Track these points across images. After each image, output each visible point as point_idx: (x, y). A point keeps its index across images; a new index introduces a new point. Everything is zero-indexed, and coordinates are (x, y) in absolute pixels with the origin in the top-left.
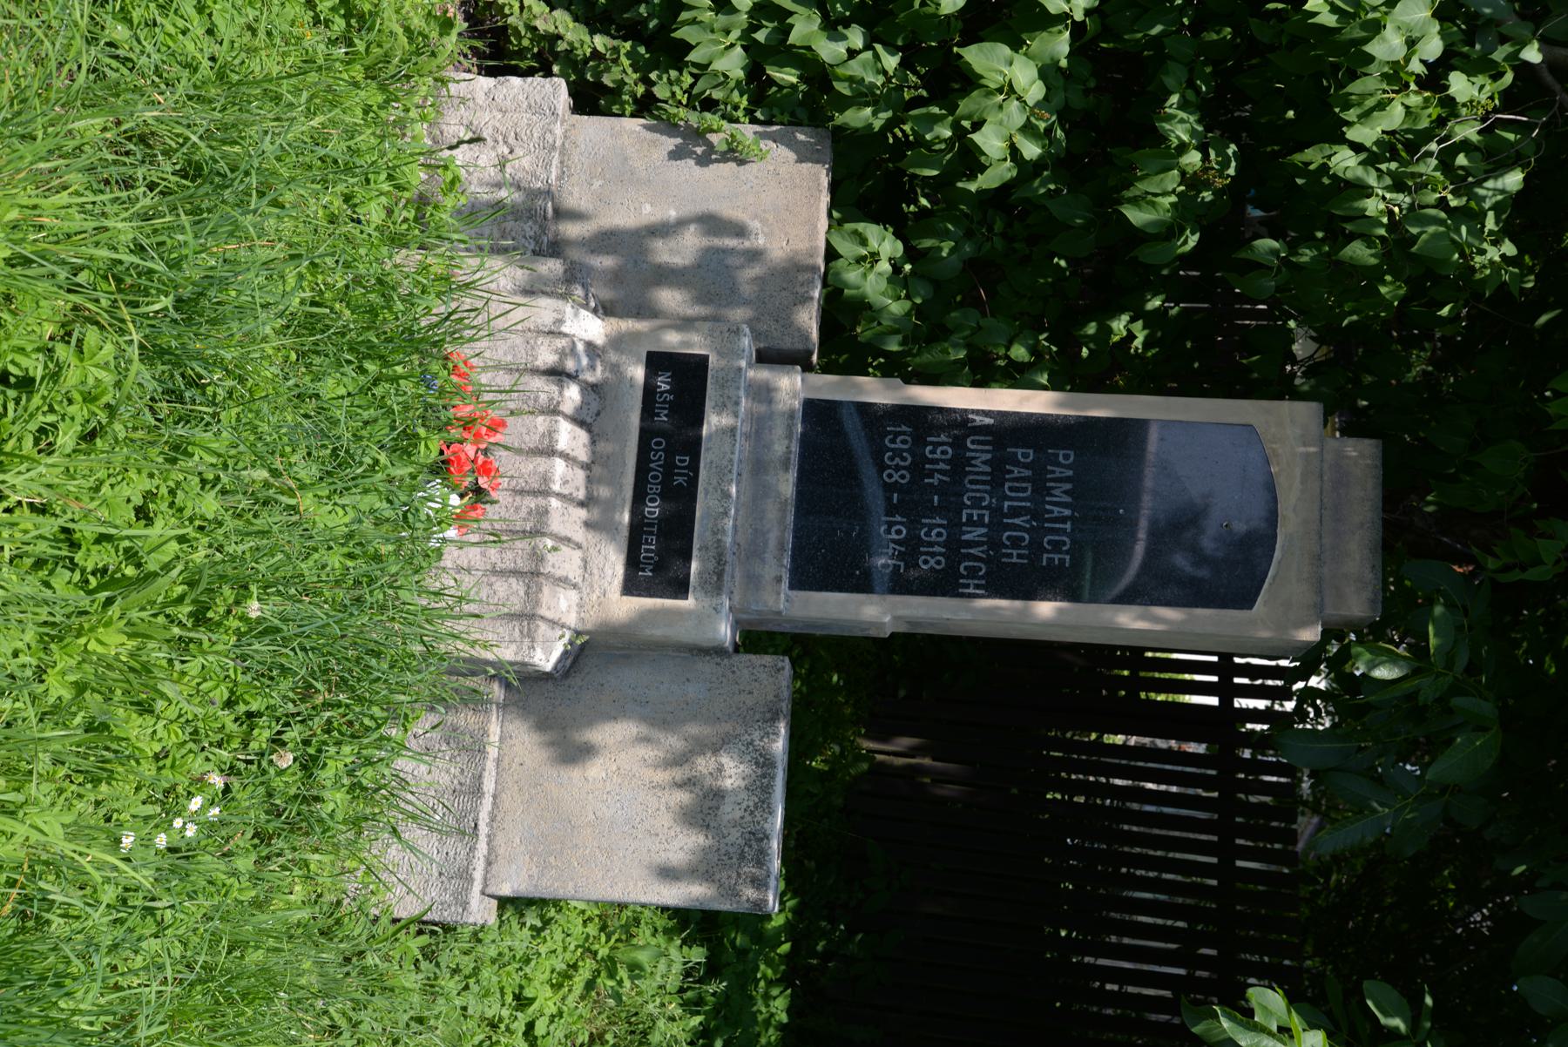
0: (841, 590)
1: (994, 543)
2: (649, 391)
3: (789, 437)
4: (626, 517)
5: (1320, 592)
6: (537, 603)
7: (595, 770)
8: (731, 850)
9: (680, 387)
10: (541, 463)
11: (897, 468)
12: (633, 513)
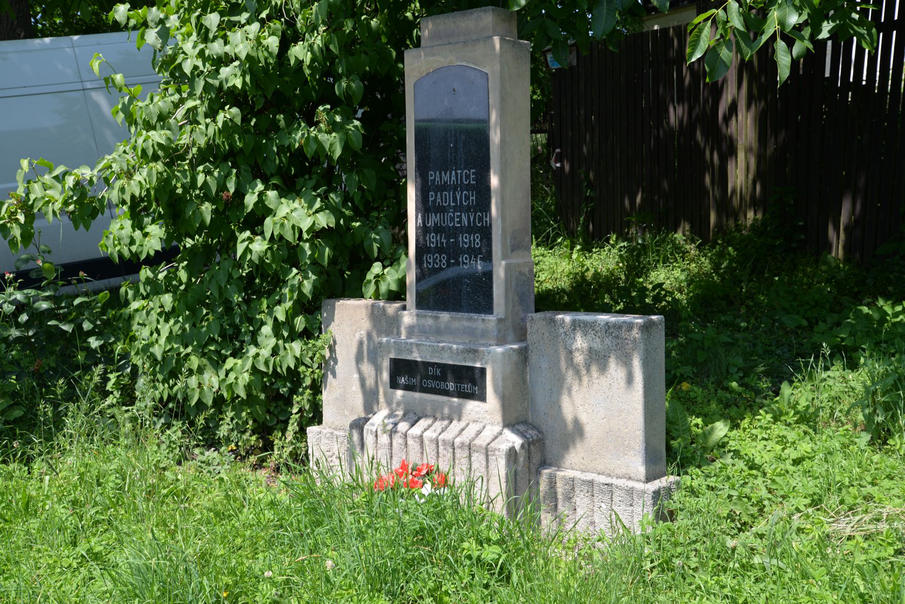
0: (491, 288)
1: (468, 209)
2: (407, 388)
3: (425, 316)
4: (455, 400)
5: (478, 40)
6: (480, 446)
7: (584, 418)
8: (614, 343)
9: (404, 372)
10: (426, 442)
11: (441, 261)
12: (453, 396)
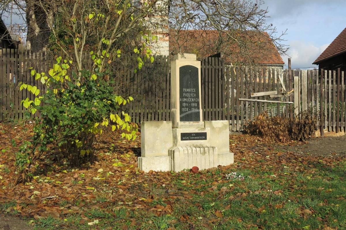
1: (194, 98)
